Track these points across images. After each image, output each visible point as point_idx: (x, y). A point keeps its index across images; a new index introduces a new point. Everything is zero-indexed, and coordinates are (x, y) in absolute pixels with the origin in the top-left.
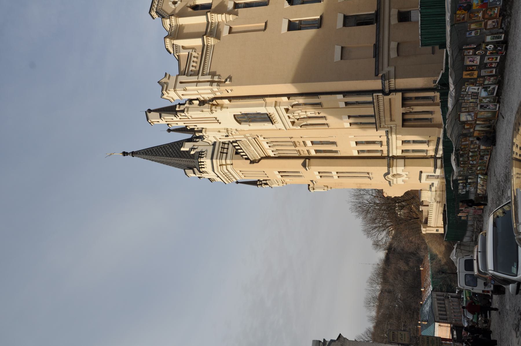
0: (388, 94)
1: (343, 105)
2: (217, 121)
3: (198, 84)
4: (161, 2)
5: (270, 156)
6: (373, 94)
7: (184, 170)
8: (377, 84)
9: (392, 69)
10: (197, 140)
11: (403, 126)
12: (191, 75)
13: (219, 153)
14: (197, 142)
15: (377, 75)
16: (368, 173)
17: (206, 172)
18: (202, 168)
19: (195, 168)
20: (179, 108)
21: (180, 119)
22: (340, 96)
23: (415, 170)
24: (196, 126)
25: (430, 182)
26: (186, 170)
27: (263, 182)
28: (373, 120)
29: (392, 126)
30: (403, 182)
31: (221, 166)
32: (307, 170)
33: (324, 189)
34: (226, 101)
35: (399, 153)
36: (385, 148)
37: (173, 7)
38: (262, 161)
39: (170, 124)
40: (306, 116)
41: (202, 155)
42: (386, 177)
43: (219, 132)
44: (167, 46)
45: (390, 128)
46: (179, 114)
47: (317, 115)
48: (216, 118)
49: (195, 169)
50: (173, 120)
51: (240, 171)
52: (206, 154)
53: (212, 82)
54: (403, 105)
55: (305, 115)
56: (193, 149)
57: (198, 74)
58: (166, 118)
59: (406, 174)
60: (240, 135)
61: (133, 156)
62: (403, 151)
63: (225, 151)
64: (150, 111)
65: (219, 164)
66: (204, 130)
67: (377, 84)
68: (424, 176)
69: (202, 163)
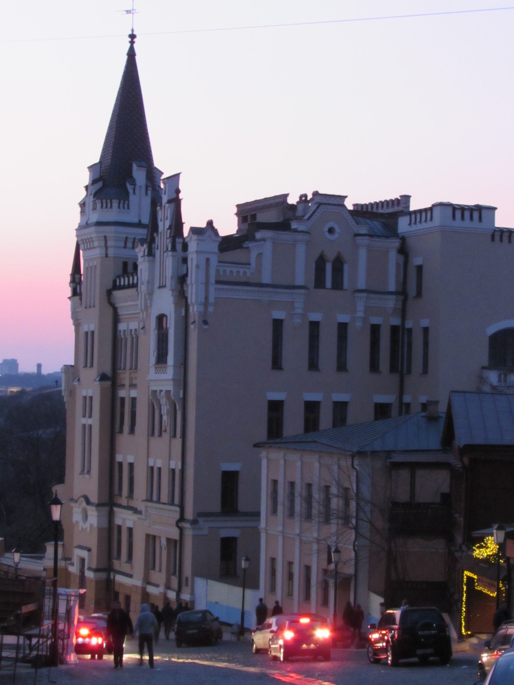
0: (177, 525)
1: (173, 466)
2: (161, 285)
5: (119, 322)
6: (179, 506)
7: (100, 162)
8: (189, 515)
9: (205, 532)
10: (149, 193)
11: (148, 536)
12: (218, 271)
13: (124, 236)
14: (147, 194)
15: (200, 515)
16: (89, 472)
19: (104, 184)
21: (167, 232)
22: (179, 467)
23: (93, 542)
24: (157, 249)
25: (76, 560)
26: (99, 166)
27: (78, 287)
28: (155, 498)
29: (148, 520)
30: (77, 522)
31: (103, 238)
32: (94, 381)
33: (65, 390)
34: (183, 314)
35: (118, 521)
36: (124, 501)
38: (110, 310)
40: (162, 413)
41: (124, 203)
42: (83, 499)
43: (148, 282)
45: (145, 518)
47: (163, 429)
48: (165, 286)
49: (99, 185)
51: (95, 266)
53: (206, 304)
54: (168, 540)
55: (164, 412)
56: (133, 187)
57: (218, 282)
58: (169, 209)
59: (86, 529)
60: (146, 304)
62: (119, 527)
63: (129, 245)
64: (178, 191)
66: (151, 258)
67: (189, 515)
68: (84, 554)
69: (109, 205)
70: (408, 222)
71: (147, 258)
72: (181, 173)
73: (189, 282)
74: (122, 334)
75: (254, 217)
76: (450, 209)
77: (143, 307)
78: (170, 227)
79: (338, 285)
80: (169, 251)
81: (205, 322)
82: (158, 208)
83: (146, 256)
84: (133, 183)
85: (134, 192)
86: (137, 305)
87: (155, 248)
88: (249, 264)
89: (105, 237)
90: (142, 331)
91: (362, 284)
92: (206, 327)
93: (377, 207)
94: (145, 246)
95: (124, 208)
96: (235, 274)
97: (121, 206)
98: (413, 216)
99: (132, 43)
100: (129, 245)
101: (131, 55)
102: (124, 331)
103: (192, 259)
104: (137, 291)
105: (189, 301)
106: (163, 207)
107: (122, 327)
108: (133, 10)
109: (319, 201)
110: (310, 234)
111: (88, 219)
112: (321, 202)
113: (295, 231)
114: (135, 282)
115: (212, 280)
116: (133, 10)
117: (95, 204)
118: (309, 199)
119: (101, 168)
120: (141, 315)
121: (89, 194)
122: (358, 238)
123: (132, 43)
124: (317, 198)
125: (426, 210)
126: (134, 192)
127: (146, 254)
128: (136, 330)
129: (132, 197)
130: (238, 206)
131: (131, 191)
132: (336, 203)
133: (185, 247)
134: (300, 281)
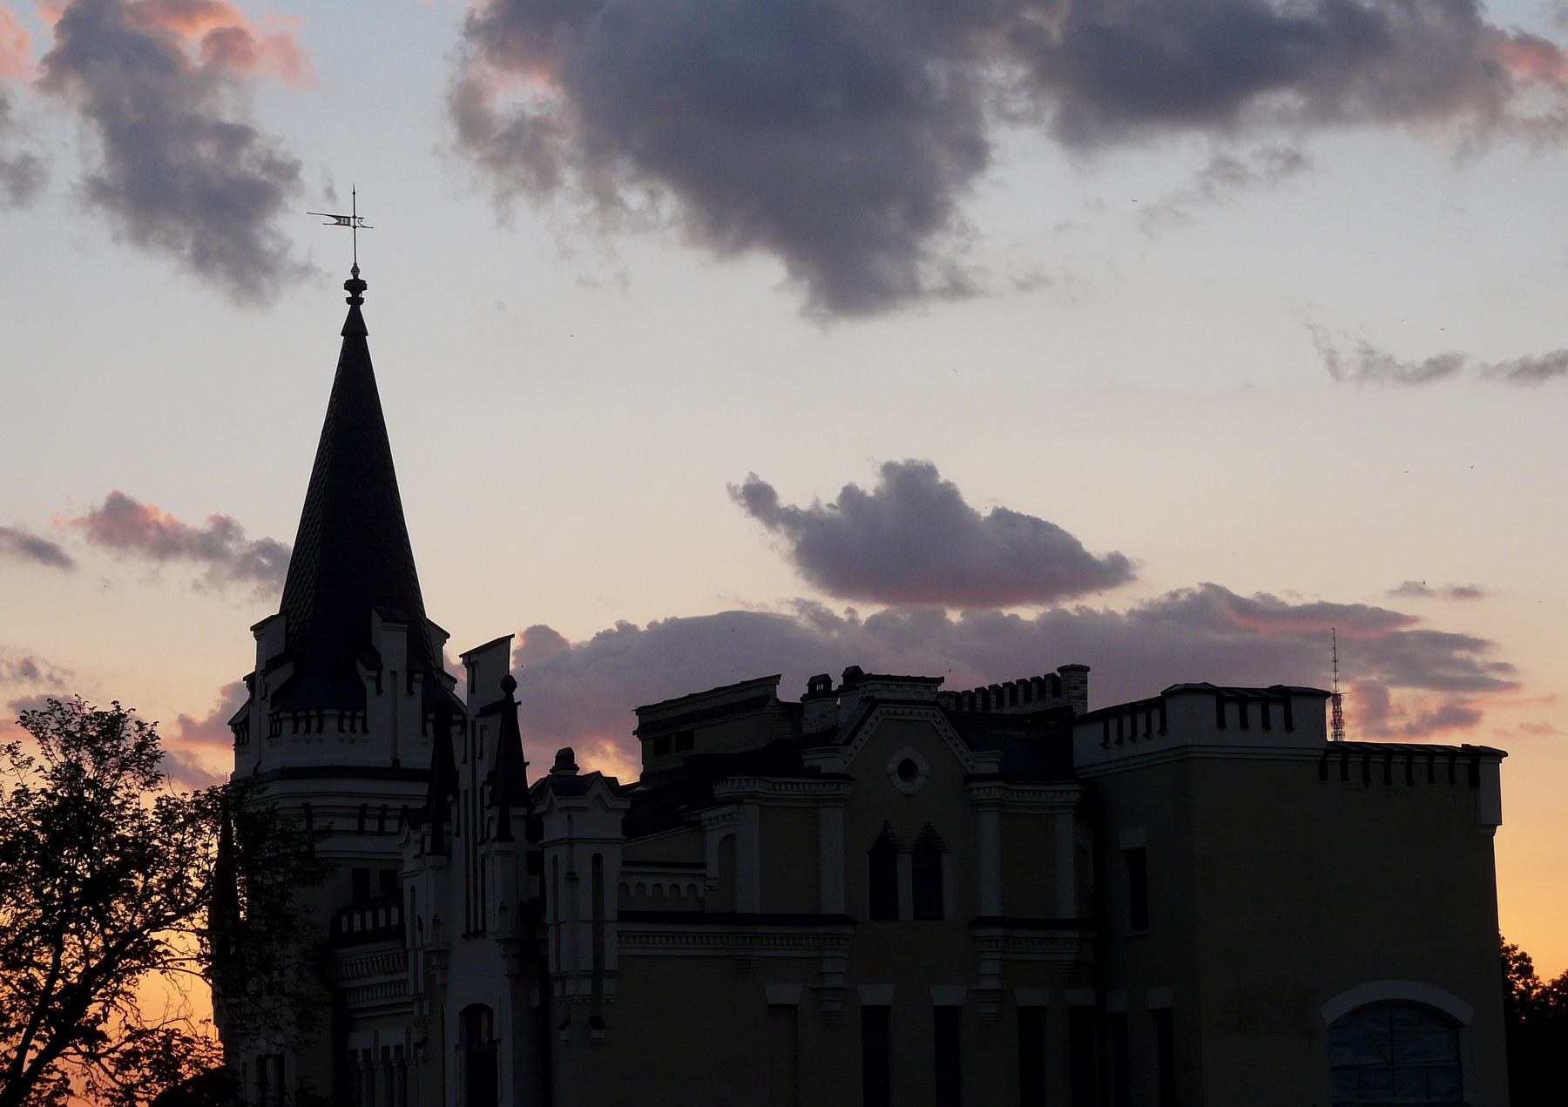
3: (590, 925)
4: (911, 712)
12: (624, 885)
13: (358, 803)
14: (410, 692)
17: (275, 734)
18: (296, 720)
20: (517, 817)
21: (482, 789)
24: (458, 835)
31: (302, 811)
34: (536, 1002)
37: (893, 766)
39: (463, 732)
43: (436, 922)
44: (733, 780)
46: (493, 812)
48: (485, 930)
49: (285, 673)
50: (478, 761)
52: (353, 742)
53: (597, 974)
56: (375, 674)
57: (624, 916)
61: (342, 334)
63: (371, 825)
65: (314, 802)
69: (314, 724)
70: (1102, 741)
71: (430, 860)
72: (513, 636)
73: (549, 918)
74: (360, 1059)
75: (686, 740)
76: (1211, 701)
77: (421, 990)
78: (490, 775)
79: (929, 905)
80: (493, 841)
81: (597, 1023)
82: (455, 730)
83: (427, 854)
84: (375, 662)
85: (379, 691)
86: (405, 982)
87: (449, 833)
88: (704, 866)
89: (307, 806)
90: (421, 1053)
91: (992, 907)
92: (596, 1034)
93: (1000, 702)
94: (425, 828)
95: (353, 729)
96: (666, 893)
97: (347, 726)
98: (1113, 724)
99: (355, 302)
100: (371, 825)
101: (355, 332)
102: (367, 1052)
103: (555, 858)
104: (404, 946)
105: (552, 969)
106: (469, 724)
107: (360, 1040)
108: (354, 217)
109: (872, 694)
110: (854, 780)
111: (259, 763)
112: (878, 696)
113: (814, 773)
114: (395, 921)
115: (610, 912)
116: (354, 217)
117: (276, 722)
118: (834, 687)
119: (288, 625)
120: (416, 1008)
121: (257, 697)
122: (975, 785)
123: (355, 302)
124: (865, 686)
125: (1147, 706)
126: (379, 691)
127: (428, 848)
128: (399, 1048)
129: (372, 700)
130: (640, 711)
131: (370, 687)
132: (914, 697)
133: (535, 828)
134: (834, 905)
